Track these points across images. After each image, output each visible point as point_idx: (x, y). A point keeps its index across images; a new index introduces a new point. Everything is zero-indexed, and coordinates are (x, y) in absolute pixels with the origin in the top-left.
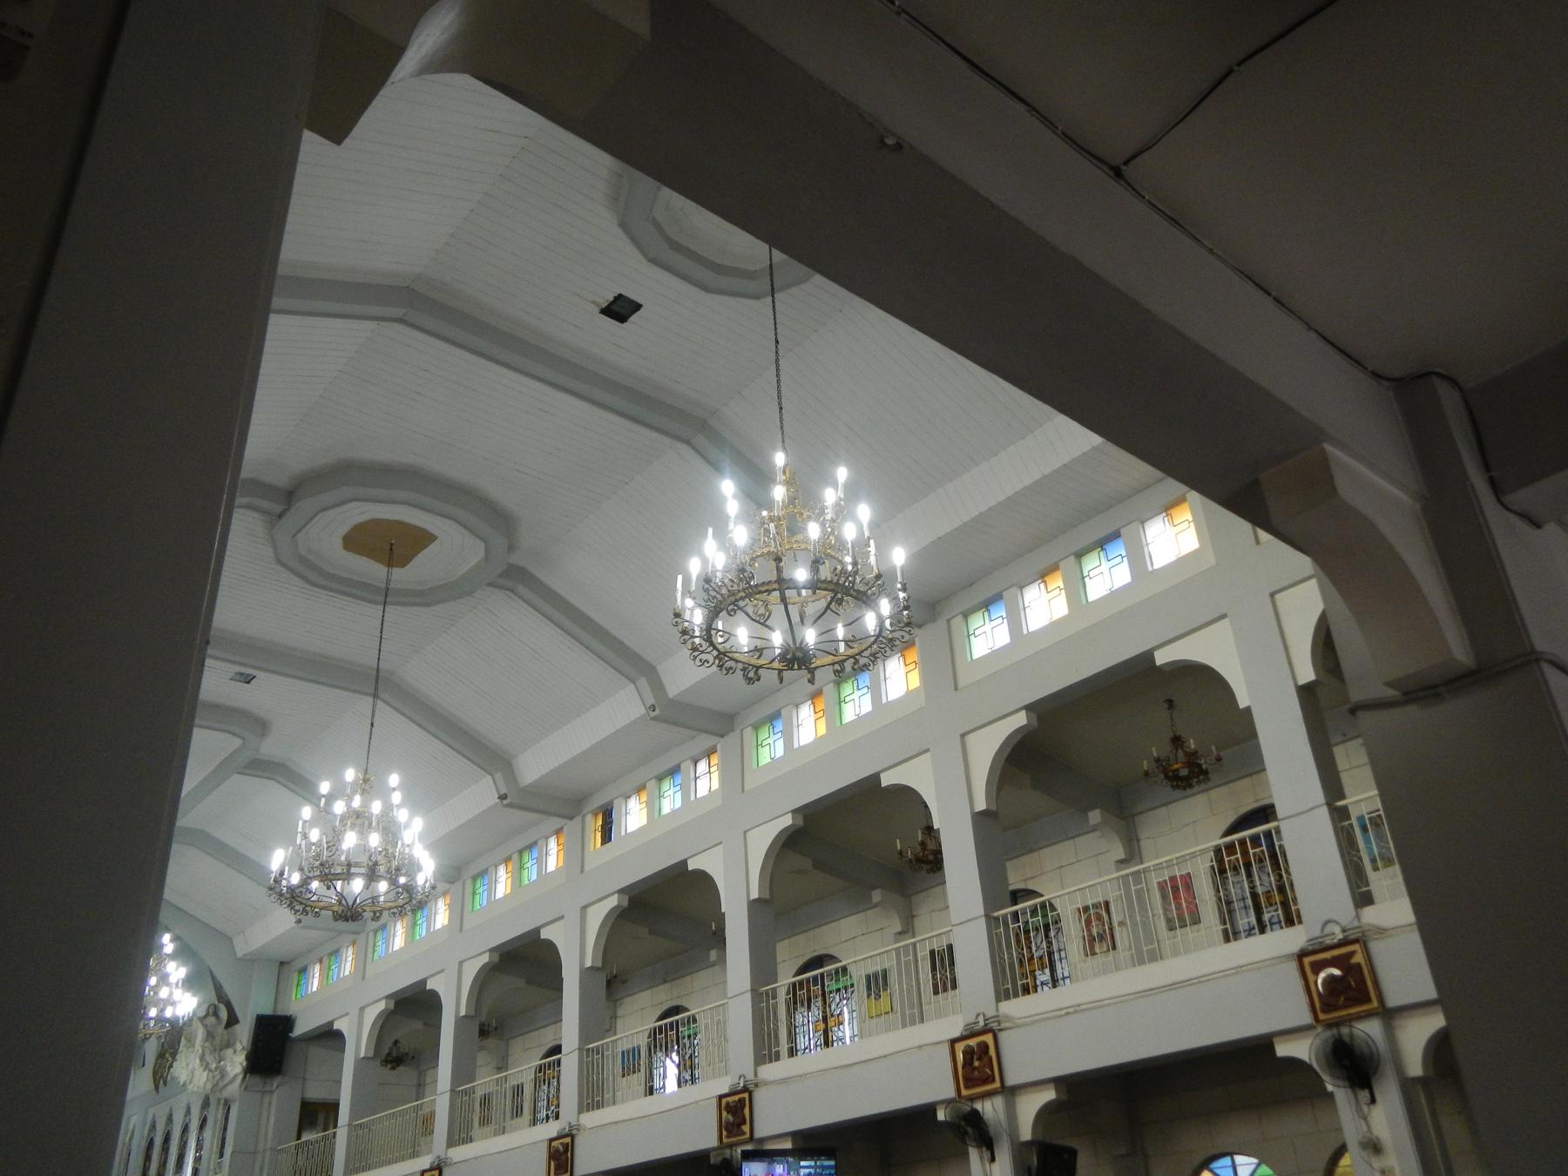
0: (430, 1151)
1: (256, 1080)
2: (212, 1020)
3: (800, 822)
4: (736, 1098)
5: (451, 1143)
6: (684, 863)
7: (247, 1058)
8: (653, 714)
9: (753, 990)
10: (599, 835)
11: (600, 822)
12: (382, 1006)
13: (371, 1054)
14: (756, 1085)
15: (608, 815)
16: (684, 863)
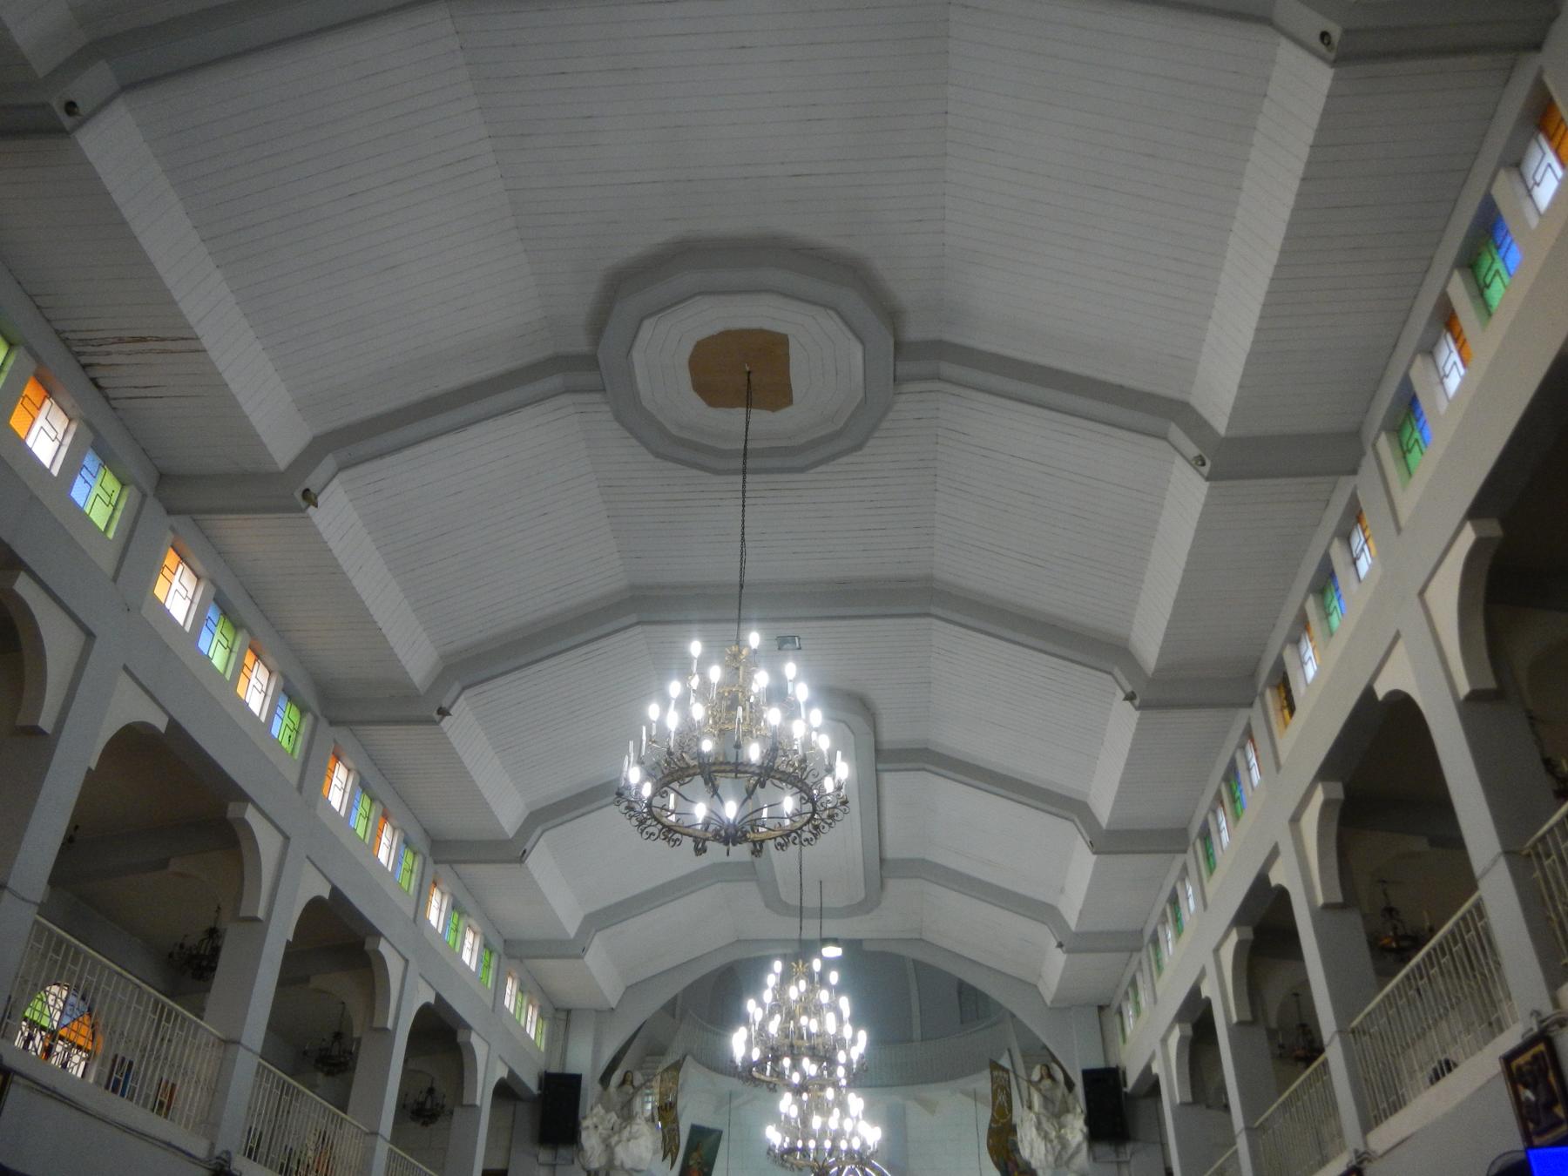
1: (1104, 1149)
2: (1047, 1082)
3: (1494, 529)
4: (1527, 1057)
6: (1369, 692)
7: (1088, 1122)
8: (1206, 470)
9: (1509, 853)
10: (1286, 712)
12: (1176, 1034)
13: (1189, 1098)
15: (1283, 684)
16: (1369, 692)
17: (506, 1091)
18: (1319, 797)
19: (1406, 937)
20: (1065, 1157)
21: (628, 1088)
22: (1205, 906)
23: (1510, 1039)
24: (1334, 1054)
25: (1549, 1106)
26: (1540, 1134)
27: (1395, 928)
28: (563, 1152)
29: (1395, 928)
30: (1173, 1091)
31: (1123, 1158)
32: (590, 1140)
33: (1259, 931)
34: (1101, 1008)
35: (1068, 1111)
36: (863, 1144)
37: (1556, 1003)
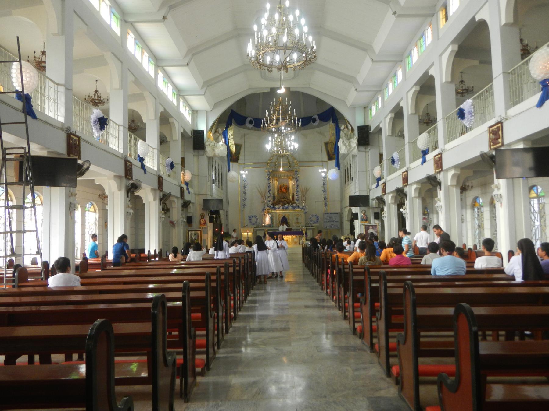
0: (405, 166)
1: (362, 148)
2: (346, 129)
4: (495, 127)
5: (410, 162)
6: (474, 18)
9: (504, 73)
10: (444, 19)
11: (444, 14)
12: (389, 116)
13: (391, 134)
14: (506, 119)
15: (446, 7)
16: (474, 18)
17: (183, 135)
18: (450, 49)
19: (465, 89)
20: (351, 150)
21: (217, 134)
22: (406, 80)
23: (492, 122)
24: (440, 124)
25: (497, 139)
26: (493, 145)
27: (462, 87)
28: (201, 152)
29: (462, 87)
30: (386, 131)
31: (367, 150)
32: (208, 148)
33: (422, 87)
34: (364, 108)
35: (351, 138)
36: (294, 148)
37: (506, 113)
